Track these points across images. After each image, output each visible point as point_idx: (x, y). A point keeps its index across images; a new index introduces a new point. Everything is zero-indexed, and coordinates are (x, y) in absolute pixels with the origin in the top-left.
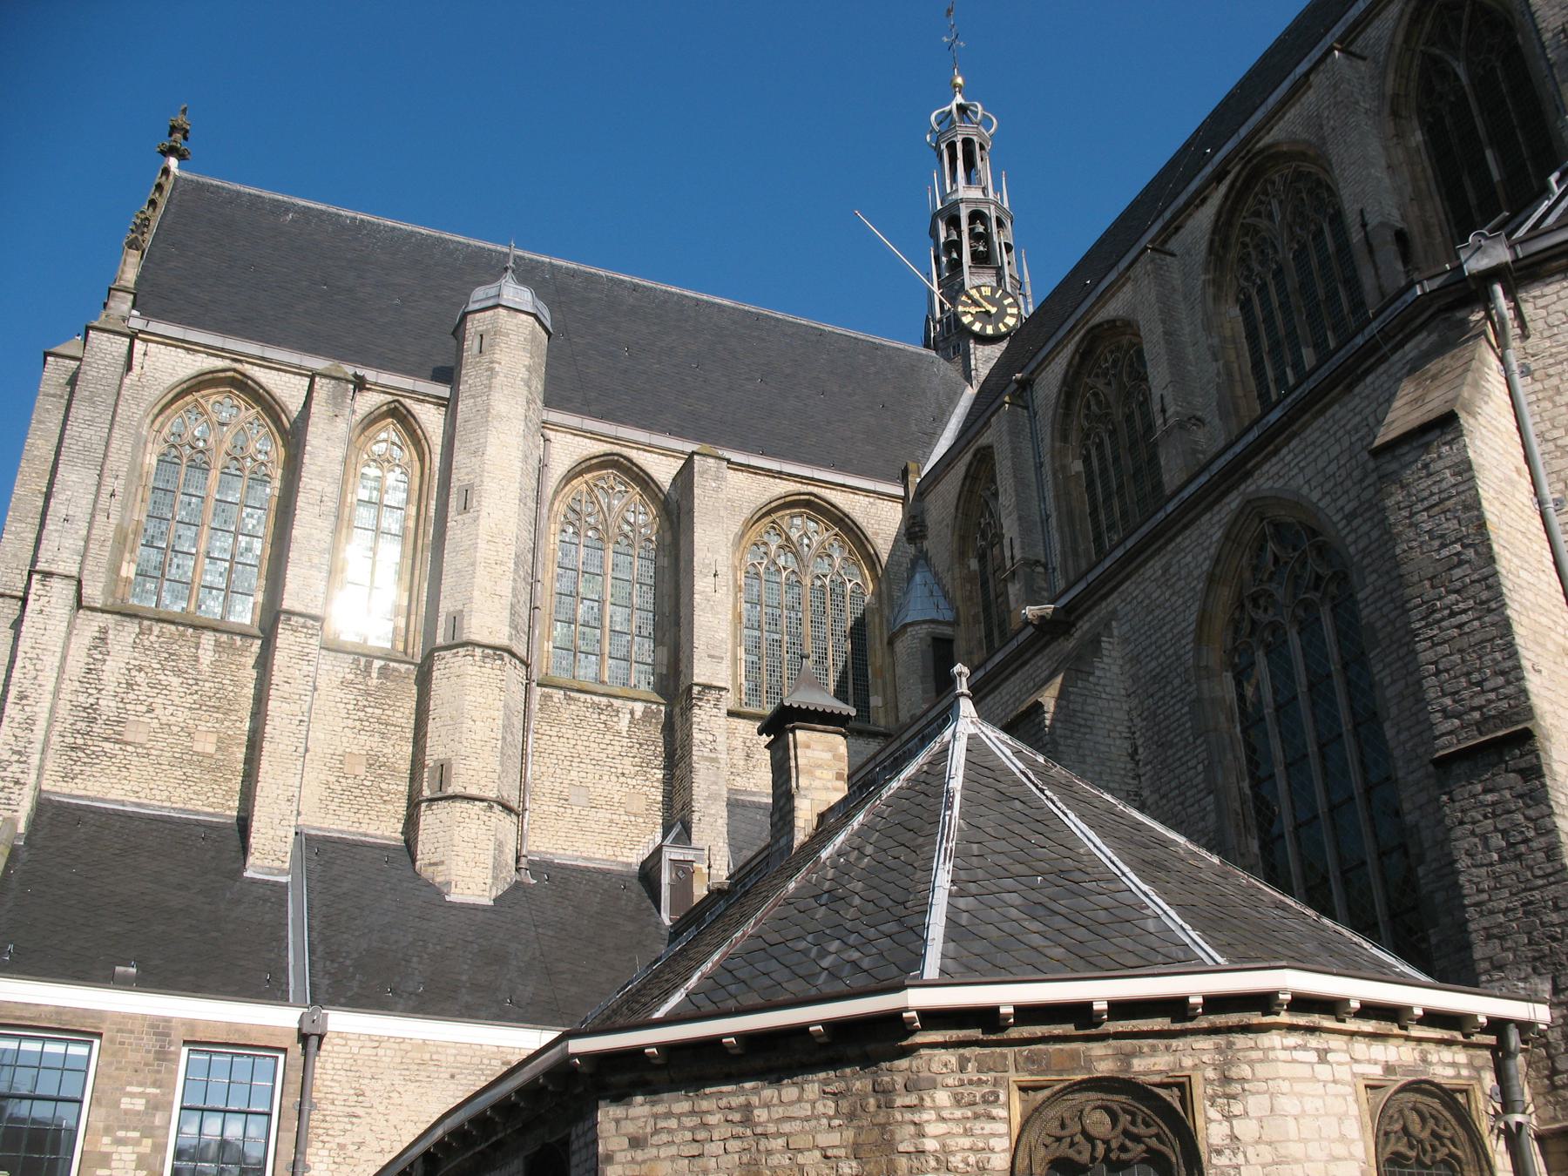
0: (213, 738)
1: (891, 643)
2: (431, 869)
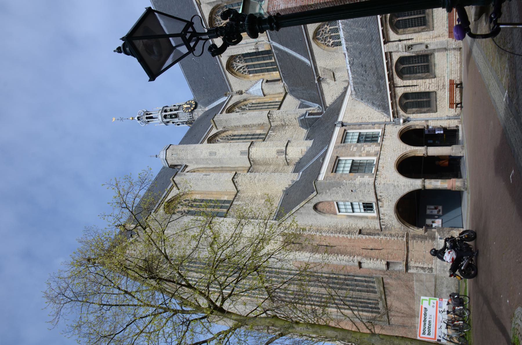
0: (261, 200)
2: (303, 153)
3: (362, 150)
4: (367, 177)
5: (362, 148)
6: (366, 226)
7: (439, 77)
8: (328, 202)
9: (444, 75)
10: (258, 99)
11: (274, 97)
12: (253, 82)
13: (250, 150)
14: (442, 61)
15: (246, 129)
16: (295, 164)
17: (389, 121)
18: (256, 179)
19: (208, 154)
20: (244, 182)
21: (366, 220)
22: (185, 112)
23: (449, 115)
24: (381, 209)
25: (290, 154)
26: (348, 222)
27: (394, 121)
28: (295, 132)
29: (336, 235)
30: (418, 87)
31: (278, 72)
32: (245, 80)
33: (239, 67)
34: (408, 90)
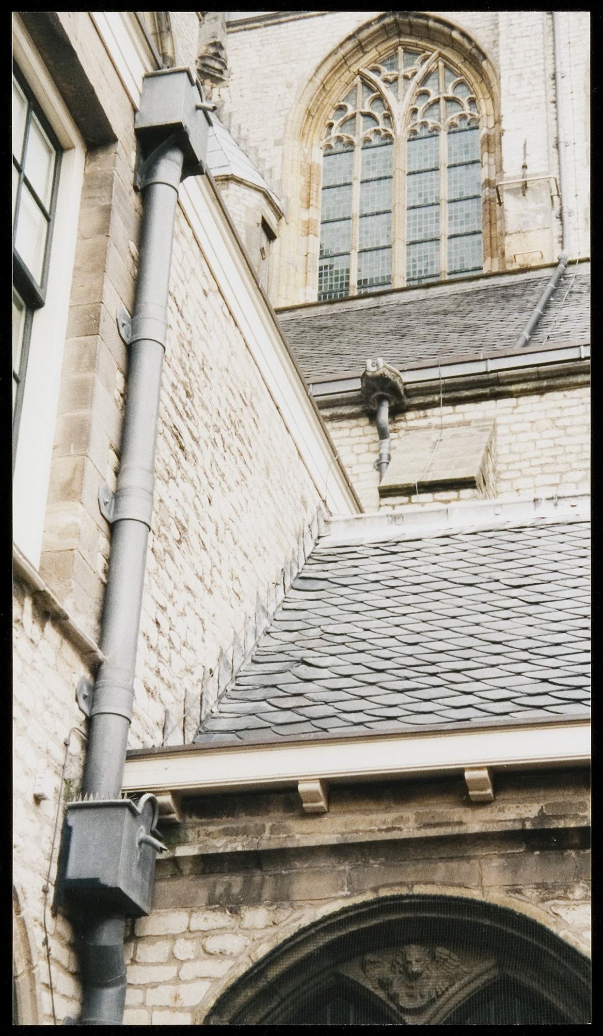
32: (298, 114)
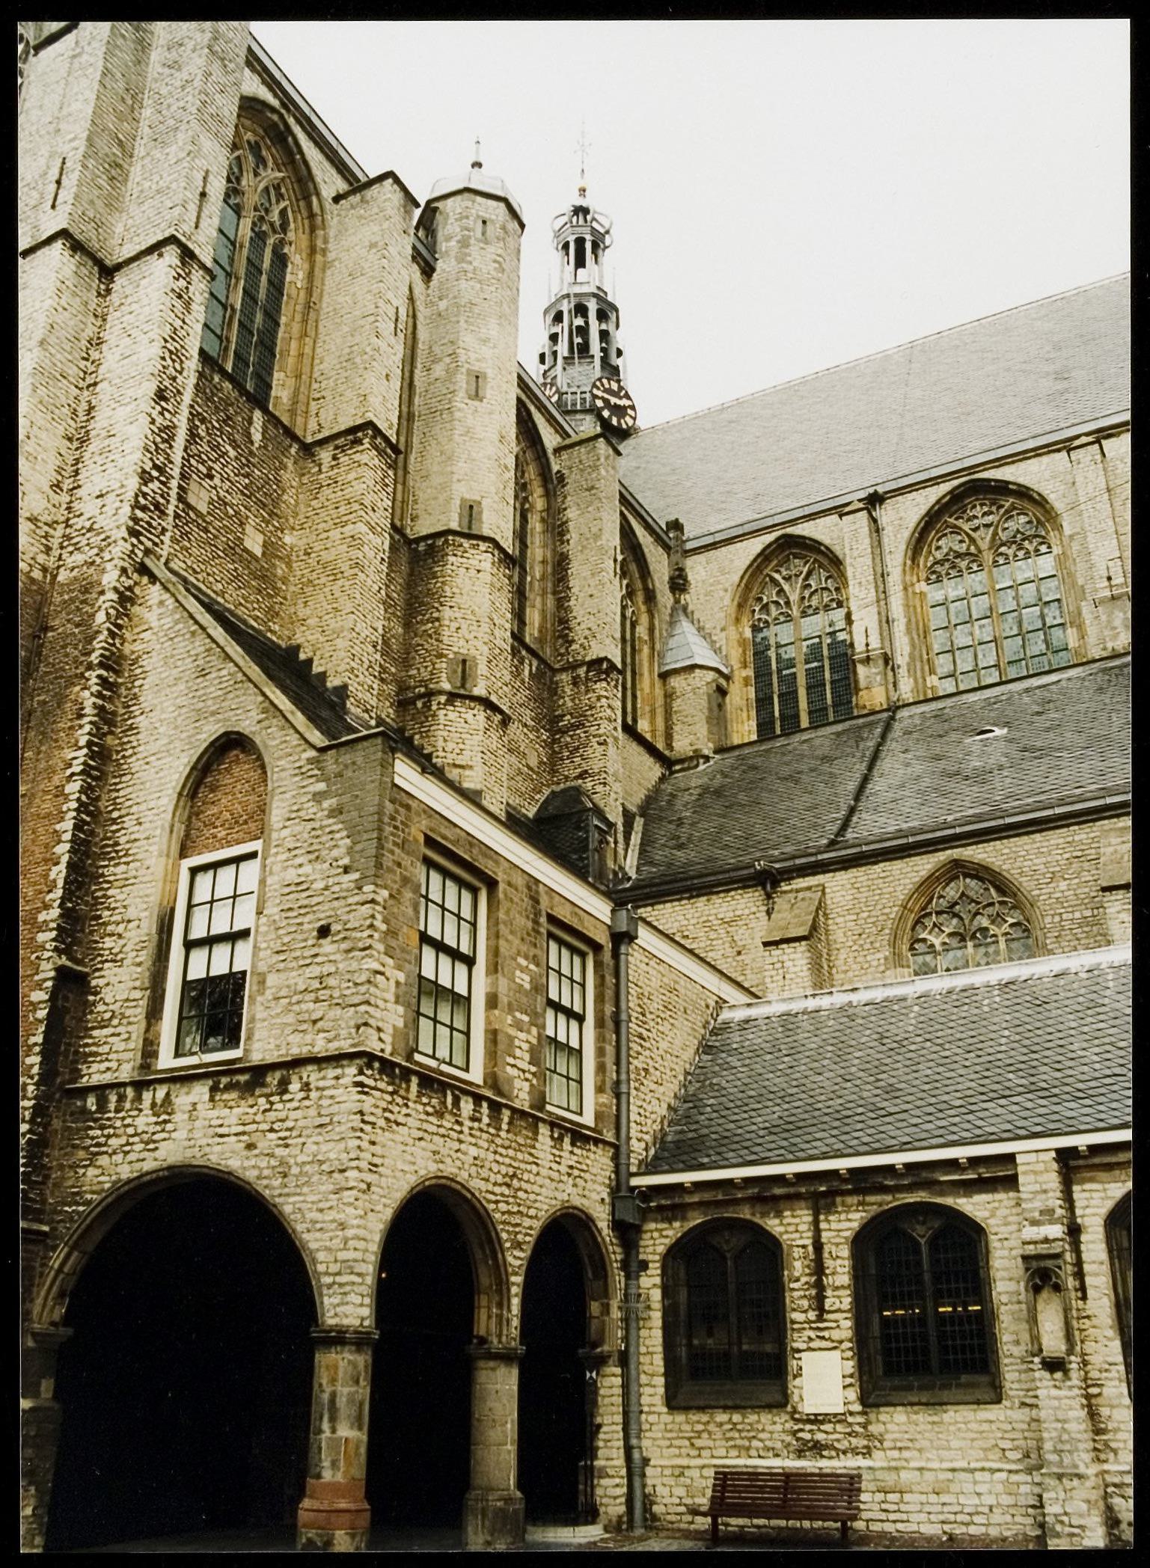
0: (260, 538)
1: (664, 676)
2: (456, 771)
3: (518, 1015)
4: (400, 1023)
5: (526, 1018)
6: (101, 1008)
7: (865, 1426)
8: (263, 809)
9: (876, 1454)
10: (653, 648)
11: (653, 712)
12: (720, 638)
13: (483, 546)
14: (955, 1444)
15: (549, 569)
16: (401, 731)
17: (633, 1169)
18: (364, 529)
19: (476, 367)
20: (352, 476)
21: (139, 1013)
22: (594, 386)
23: (649, 1471)
24: (200, 1091)
25: (452, 716)
26: (131, 913)
27: (633, 1189)
28: (528, 767)
29: (63, 849)
30: (812, 1315)
31: (754, 737)
32: (732, 610)
33: (786, 587)
34: (798, 1264)
